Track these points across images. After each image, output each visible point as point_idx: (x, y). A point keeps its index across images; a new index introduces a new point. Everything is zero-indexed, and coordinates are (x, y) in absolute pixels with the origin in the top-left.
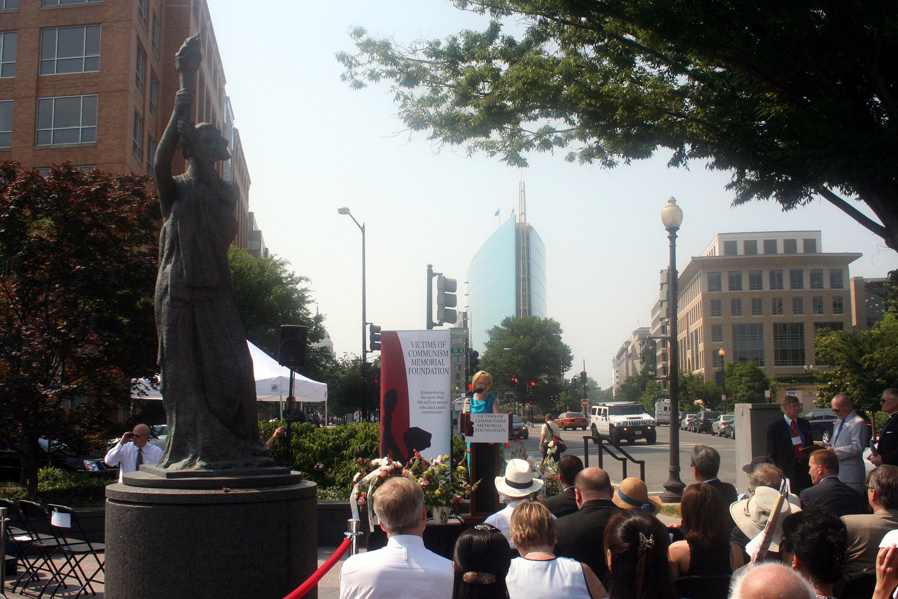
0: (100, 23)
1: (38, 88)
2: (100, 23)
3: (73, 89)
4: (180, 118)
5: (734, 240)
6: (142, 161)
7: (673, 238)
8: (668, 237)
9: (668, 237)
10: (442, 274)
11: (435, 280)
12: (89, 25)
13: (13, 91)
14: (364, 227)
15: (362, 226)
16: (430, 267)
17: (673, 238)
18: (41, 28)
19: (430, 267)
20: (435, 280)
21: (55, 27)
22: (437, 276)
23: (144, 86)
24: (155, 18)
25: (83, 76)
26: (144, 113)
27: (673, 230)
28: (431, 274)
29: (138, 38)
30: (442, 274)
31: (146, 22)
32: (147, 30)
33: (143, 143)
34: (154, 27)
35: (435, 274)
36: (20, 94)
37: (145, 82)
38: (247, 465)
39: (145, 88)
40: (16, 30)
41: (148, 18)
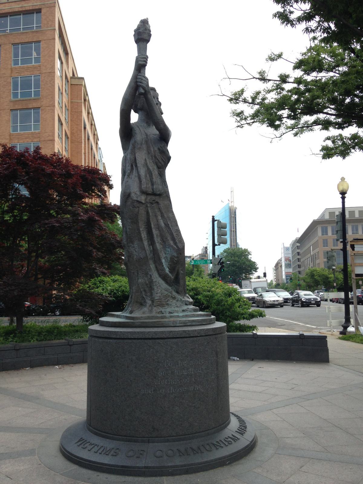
0: (40, 107)
1: (10, 139)
3: (28, 140)
4: (140, 74)
5: (334, 211)
7: (343, 198)
8: (341, 197)
9: (341, 197)
10: (219, 220)
16: (213, 217)
17: (343, 198)
18: (11, 110)
20: (216, 223)
21: (18, 109)
22: (217, 221)
23: (62, 138)
24: (66, 106)
25: (32, 133)
26: (62, 152)
27: (343, 194)
28: (214, 220)
29: (58, 115)
30: (219, 220)
31: (62, 107)
32: (63, 112)
34: (65, 112)
35: (216, 220)
37: (62, 137)
38: (183, 311)
39: (62, 140)
41: (62, 106)
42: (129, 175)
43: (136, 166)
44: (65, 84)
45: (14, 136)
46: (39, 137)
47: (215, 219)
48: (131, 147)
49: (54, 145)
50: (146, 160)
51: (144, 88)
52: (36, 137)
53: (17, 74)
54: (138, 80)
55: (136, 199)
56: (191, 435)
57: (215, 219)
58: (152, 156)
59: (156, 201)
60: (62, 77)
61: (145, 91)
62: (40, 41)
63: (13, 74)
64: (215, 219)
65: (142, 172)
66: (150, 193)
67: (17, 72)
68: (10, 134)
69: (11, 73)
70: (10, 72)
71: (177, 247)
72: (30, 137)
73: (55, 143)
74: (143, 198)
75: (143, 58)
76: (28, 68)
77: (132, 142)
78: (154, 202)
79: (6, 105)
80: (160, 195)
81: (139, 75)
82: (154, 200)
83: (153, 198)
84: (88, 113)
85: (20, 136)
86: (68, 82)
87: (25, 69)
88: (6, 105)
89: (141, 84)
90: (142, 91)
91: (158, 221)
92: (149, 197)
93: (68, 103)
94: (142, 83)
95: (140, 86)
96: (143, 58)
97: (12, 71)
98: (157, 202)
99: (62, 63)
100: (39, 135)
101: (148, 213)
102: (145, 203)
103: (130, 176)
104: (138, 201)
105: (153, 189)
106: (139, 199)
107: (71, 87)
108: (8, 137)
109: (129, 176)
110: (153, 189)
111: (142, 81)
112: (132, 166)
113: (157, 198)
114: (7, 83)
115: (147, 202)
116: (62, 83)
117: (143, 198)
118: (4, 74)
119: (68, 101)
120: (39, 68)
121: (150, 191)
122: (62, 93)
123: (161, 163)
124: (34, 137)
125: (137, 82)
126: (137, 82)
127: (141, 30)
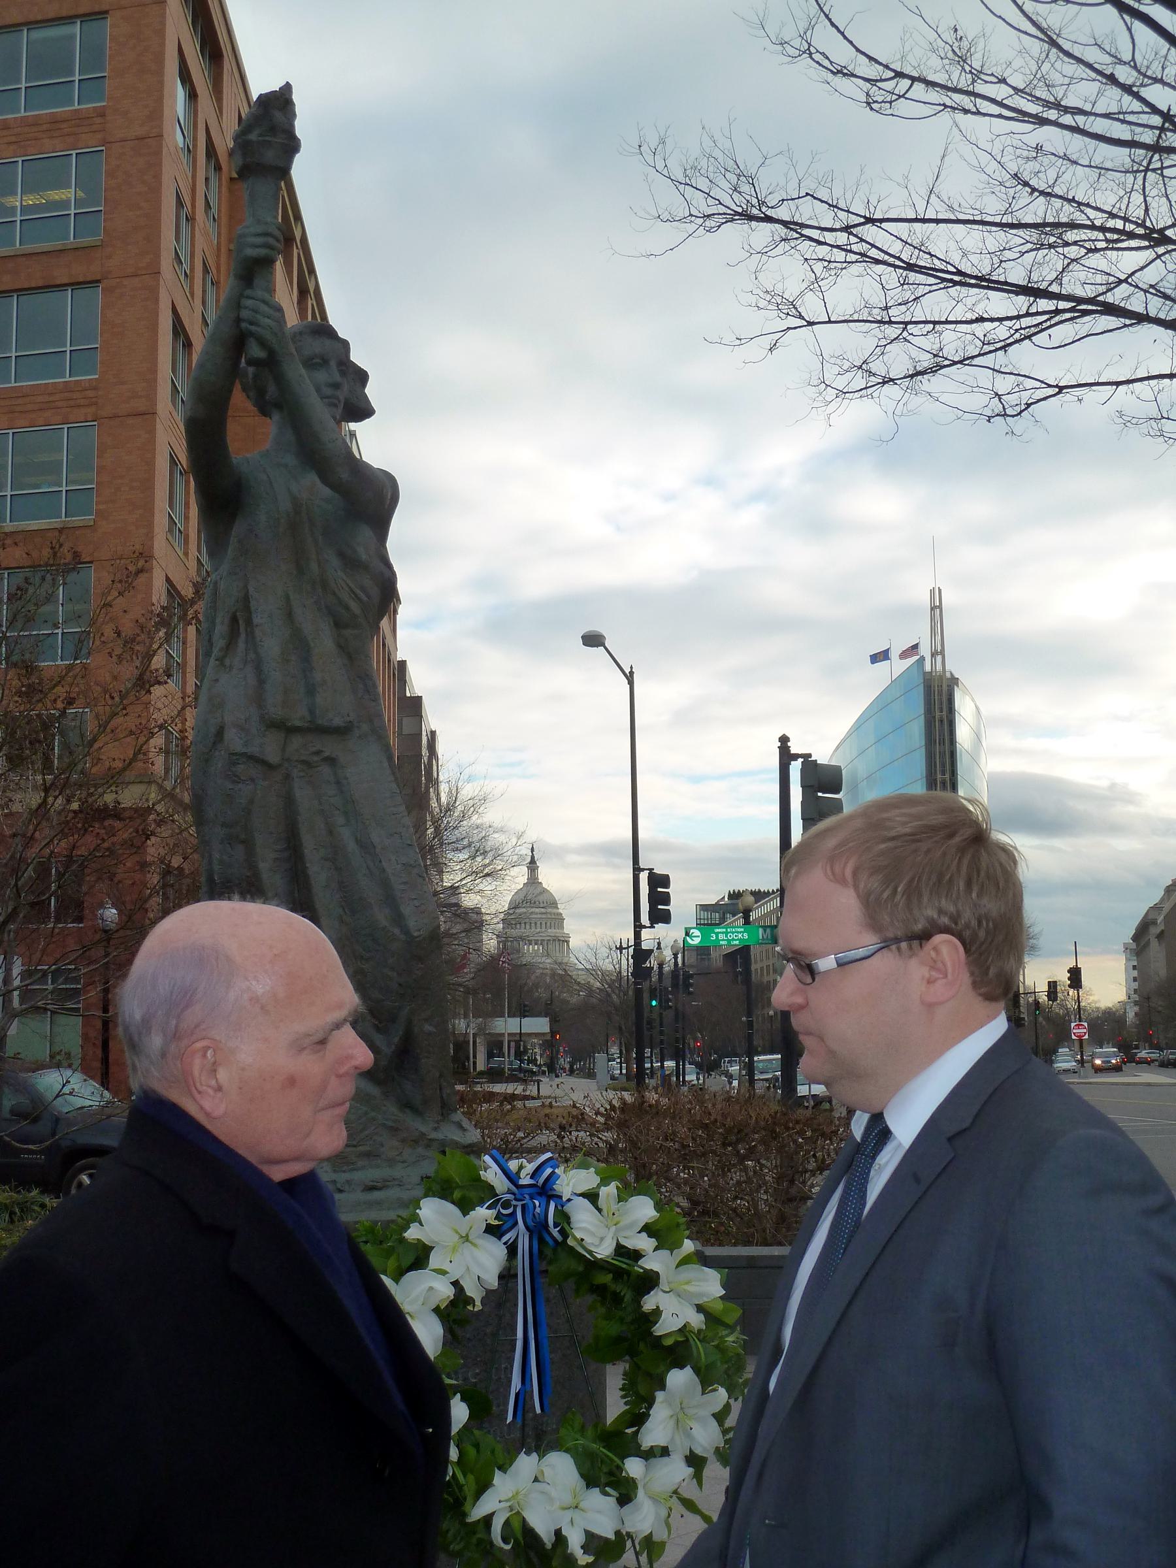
0: (98, 281)
2: (98, 281)
4: (248, 292)
6: (186, 554)
11: (795, 768)
12: (76, 285)
14: (631, 673)
15: (627, 671)
16: (784, 740)
19: (784, 740)
20: (795, 768)
22: (800, 760)
24: (206, 270)
28: (786, 756)
33: (187, 518)
34: (204, 291)
35: (796, 757)
41: (192, 269)
42: (224, 657)
43: (249, 622)
44: (207, 179)
46: (96, 404)
47: (792, 752)
48: (230, 551)
49: (152, 431)
50: (287, 598)
51: (262, 343)
52: (82, 402)
53: (12, 147)
54: (245, 314)
55: (244, 750)
57: (793, 751)
60: (190, 151)
61: (272, 353)
62: (106, 12)
64: (793, 751)
65: (271, 645)
66: (298, 723)
67: (13, 139)
71: (406, 932)
72: (60, 404)
73: (159, 426)
74: (270, 747)
75: (259, 235)
76: (55, 121)
77: (239, 528)
78: (316, 758)
80: (342, 732)
81: (248, 297)
82: (318, 753)
84: (303, 292)
85: (20, 401)
86: (218, 168)
87: (45, 127)
89: (253, 328)
90: (256, 351)
91: (331, 833)
92: (296, 741)
93: (218, 256)
94: (259, 326)
95: (251, 334)
96: (259, 235)
98: (331, 761)
99: (192, 96)
100: (90, 394)
101: (289, 801)
103: (227, 662)
104: (251, 758)
105: (311, 711)
106: (254, 750)
107: (230, 191)
109: (221, 660)
110: (311, 711)
111: (258, 316)
112: (234, 620)
113: (330, 746)
115: (288, 760)
116: (194, 177)
117: (270, 747)
119: (219, 249)
120: (98, 120)
121: (298, 717)
122: (190, 219)
123: (347, 608)
124: (72, 403)
125: (238, 320)
126: (238, 320)
127: (253, 137)
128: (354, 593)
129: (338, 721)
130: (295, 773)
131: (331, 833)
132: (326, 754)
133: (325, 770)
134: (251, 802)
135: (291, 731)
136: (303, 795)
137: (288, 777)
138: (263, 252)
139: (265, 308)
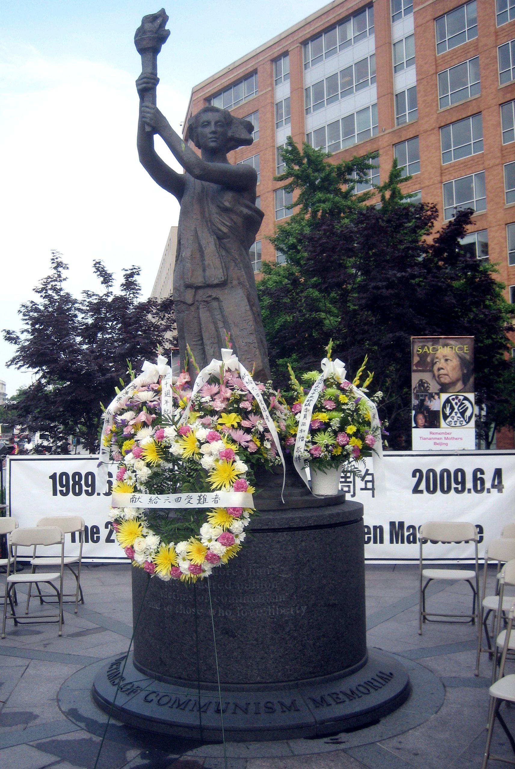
1: (503, 156)
13: (483, 163)
21: (511, 100)
36: (489, 165)
40: (481, 112)
45: (507, 150)
53: (507, 37)
55: (179, 299)
56: (210, 684)
58: (207, 221)
59: (213, 297)
63: (498, 41)
66: (200, 285)
67: (506, 34)
68: (502, 147)
69: (496, 40)
70: (493, 38)
78: (210, 299)
79: (492, 99)
82: (210, 296)
83: (210, 292)
88: (492, 99)
92: (201, 292)
97: (497, 36)
98: (217, 299)
102: (193, 304)
104: (181, 302)
108: (499, 154)
110: (204, 277)
113: (215, 293)
114: (490, 61)
115: (197, 301)
118: (486, 45)
121: (199, 280)
123: (220, 230)
128: (223, 222)
129: (216, 282)
130: (201, 306)
131: (217, 331)
132: (214, 296)
133: (215, 304)
134: (183, 321)
135: (197, 288)
136: (204, 315)
137: (198, 308)
138: (144, 85)
139: (148, 110)
